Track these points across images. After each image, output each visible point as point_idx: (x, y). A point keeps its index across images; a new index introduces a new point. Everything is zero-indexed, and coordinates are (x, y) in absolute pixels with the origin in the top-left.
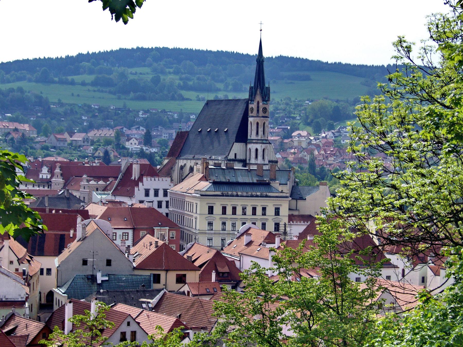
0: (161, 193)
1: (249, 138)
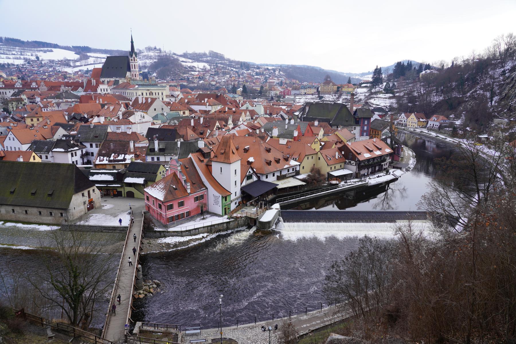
0: (105, 90)
1: (131, 69)
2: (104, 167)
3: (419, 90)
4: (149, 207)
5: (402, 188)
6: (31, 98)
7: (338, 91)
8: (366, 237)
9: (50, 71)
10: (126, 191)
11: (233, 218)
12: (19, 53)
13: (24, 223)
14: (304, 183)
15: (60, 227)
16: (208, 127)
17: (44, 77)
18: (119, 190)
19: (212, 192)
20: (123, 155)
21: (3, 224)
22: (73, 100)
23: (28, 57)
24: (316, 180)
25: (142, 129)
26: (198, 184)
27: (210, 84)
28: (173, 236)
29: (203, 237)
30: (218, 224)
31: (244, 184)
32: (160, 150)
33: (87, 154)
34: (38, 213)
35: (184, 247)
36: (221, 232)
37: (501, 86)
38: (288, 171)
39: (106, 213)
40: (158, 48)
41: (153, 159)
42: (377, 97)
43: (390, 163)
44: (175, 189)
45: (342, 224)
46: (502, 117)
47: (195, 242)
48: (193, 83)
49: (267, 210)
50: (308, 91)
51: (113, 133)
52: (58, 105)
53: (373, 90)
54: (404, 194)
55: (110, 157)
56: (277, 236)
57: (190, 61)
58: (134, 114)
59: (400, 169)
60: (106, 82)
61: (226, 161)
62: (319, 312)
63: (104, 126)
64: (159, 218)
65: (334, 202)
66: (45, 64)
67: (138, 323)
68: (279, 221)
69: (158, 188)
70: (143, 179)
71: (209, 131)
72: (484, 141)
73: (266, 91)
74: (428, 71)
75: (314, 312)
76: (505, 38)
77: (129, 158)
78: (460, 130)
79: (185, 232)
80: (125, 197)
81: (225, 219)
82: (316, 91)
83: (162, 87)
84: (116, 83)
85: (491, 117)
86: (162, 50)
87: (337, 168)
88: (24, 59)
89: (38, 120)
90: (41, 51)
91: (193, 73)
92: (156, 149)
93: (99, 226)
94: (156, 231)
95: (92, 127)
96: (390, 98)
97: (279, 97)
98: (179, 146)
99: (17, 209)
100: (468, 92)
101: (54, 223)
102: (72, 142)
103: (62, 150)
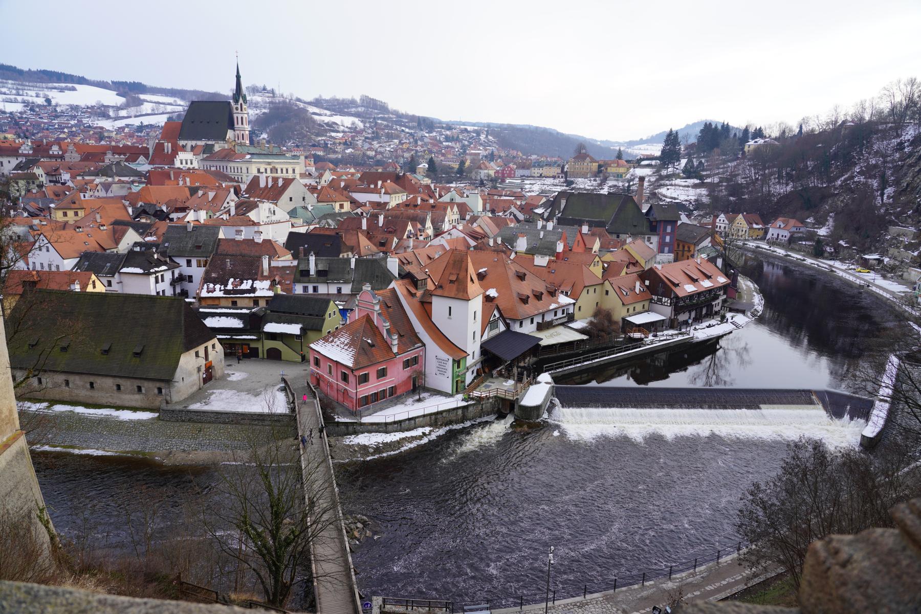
0: (189, 162)
1: (236, 126)
2: (216, 302)
3: (746, 173)
4: (318, 380)
5: (743, 345)
6: (53, 174)
7: (601, 172)
8: (820, 440)
9: (72, 126)
10: (266, 348)
11: (472, 399)
12: (14, 92)
13: (87, 405)
14: (585, 337)
15: (156, 415)
16: (393, 232)
17: (62, 136)
18: (253, 345)
19: (433, 351)
20: (250, 282)
21: (48, 408)
22: (132, 178)
23: (30, 99)
24: (604, 332)
25: (279, 234)
26: (410, 338)
27: (364, 154)
28: (370, 432)
29: (424, 434)
30: (448, 411)
31: (485, 337)
32: (319, 273)
33: (181, 278)
34: (115, 388)
35: (392, 453)
36: (454, 425)
37: (897, 169)
38: (555, 315)
39: (237, 387)
40: (269, 88)
41: (305, 289)
42: (671, 185)
43: (724, 301)
44: (369, 345)
45: (667, 411)
46: (904, 223)
47: (411, 442)
48: (335, 152)
49: (531, 384)
50: (545, 171)
51: (226, 240)
52: (107, 187)
53: (664, 172)
54: (746, 357)
55: (226, 285)
56: (556, 433)
57: (328, 113)
58: (258, 206)
59: (743, 312)
60: (189, 147)
61: (460, 296)
62: (691, 574)
63: (212, 228)
64: (341, 399)
65: (629, 371)
66: (62, 112)
67: (374, 598)
68: (553, 405)
69: (338, 343)
70: (300, 326)
71: (395, 239)
72: (874, 266)
73: (470, 169)
74: (761, 141)
75: (684, 574)
76: (902, 86)
77: (263, 289)
78: (828, 245)
79: (394, 424)
80: (263, 358)
81: (457, 402)
82: (559, 171)
83: (295, 157)
84: (208, 149)
85: (884, 223)
86: (277, 92)
87: (637, 310)
88: (24, 102)
89: (76, 214)
90: (55, 88)
91: (333, 134)
92: (312, 272)
93: (234, 413)
94: (338, 422)
95: (190, 229)
96: (695, 186)
97: (493, 180)
98: (353, 266)
99: (75, 380)
100: (838, 178)
101: (143, 405)
102: (156, 256)
103: (139, 270)
